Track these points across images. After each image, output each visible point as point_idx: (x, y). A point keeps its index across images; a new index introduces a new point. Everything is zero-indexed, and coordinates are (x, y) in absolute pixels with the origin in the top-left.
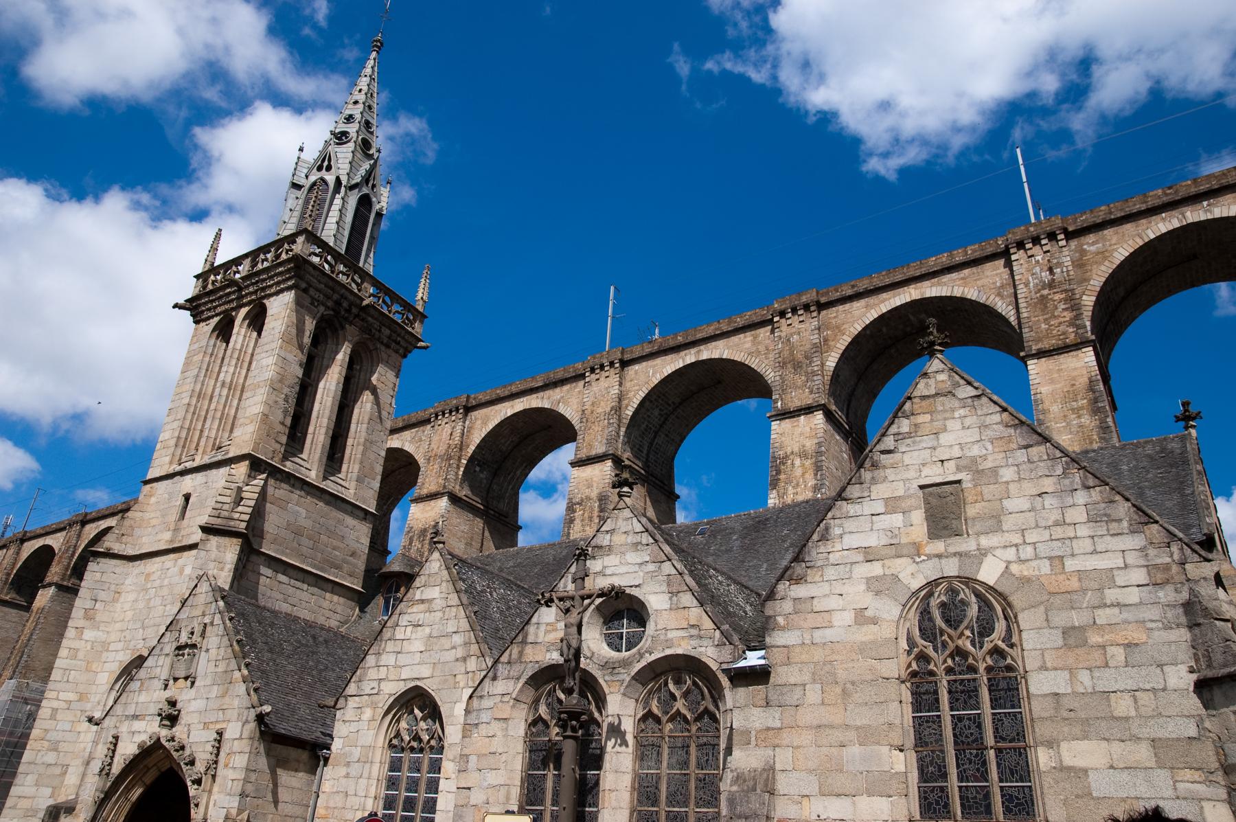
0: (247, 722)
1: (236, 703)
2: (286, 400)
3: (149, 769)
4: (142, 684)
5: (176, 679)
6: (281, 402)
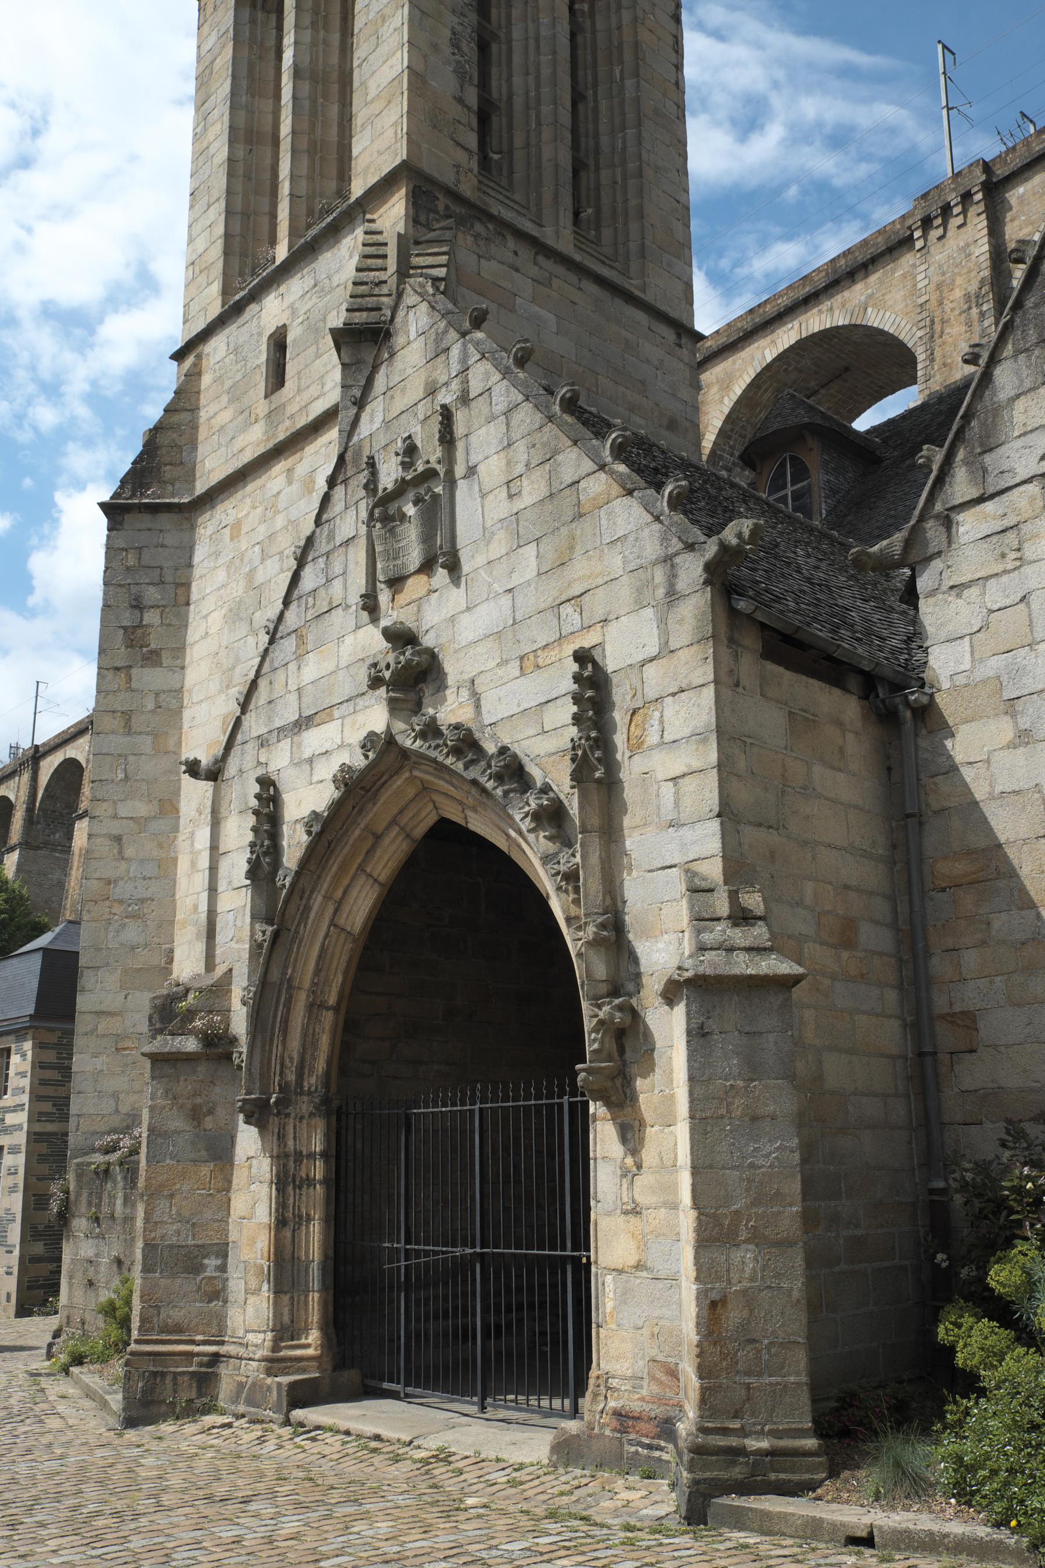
0: (673, 596)
1: (615, 562)
2: (455, 43)
3: (378, 838)
4: (301, 640)
5: (396, 583)
6: (448, 50)
